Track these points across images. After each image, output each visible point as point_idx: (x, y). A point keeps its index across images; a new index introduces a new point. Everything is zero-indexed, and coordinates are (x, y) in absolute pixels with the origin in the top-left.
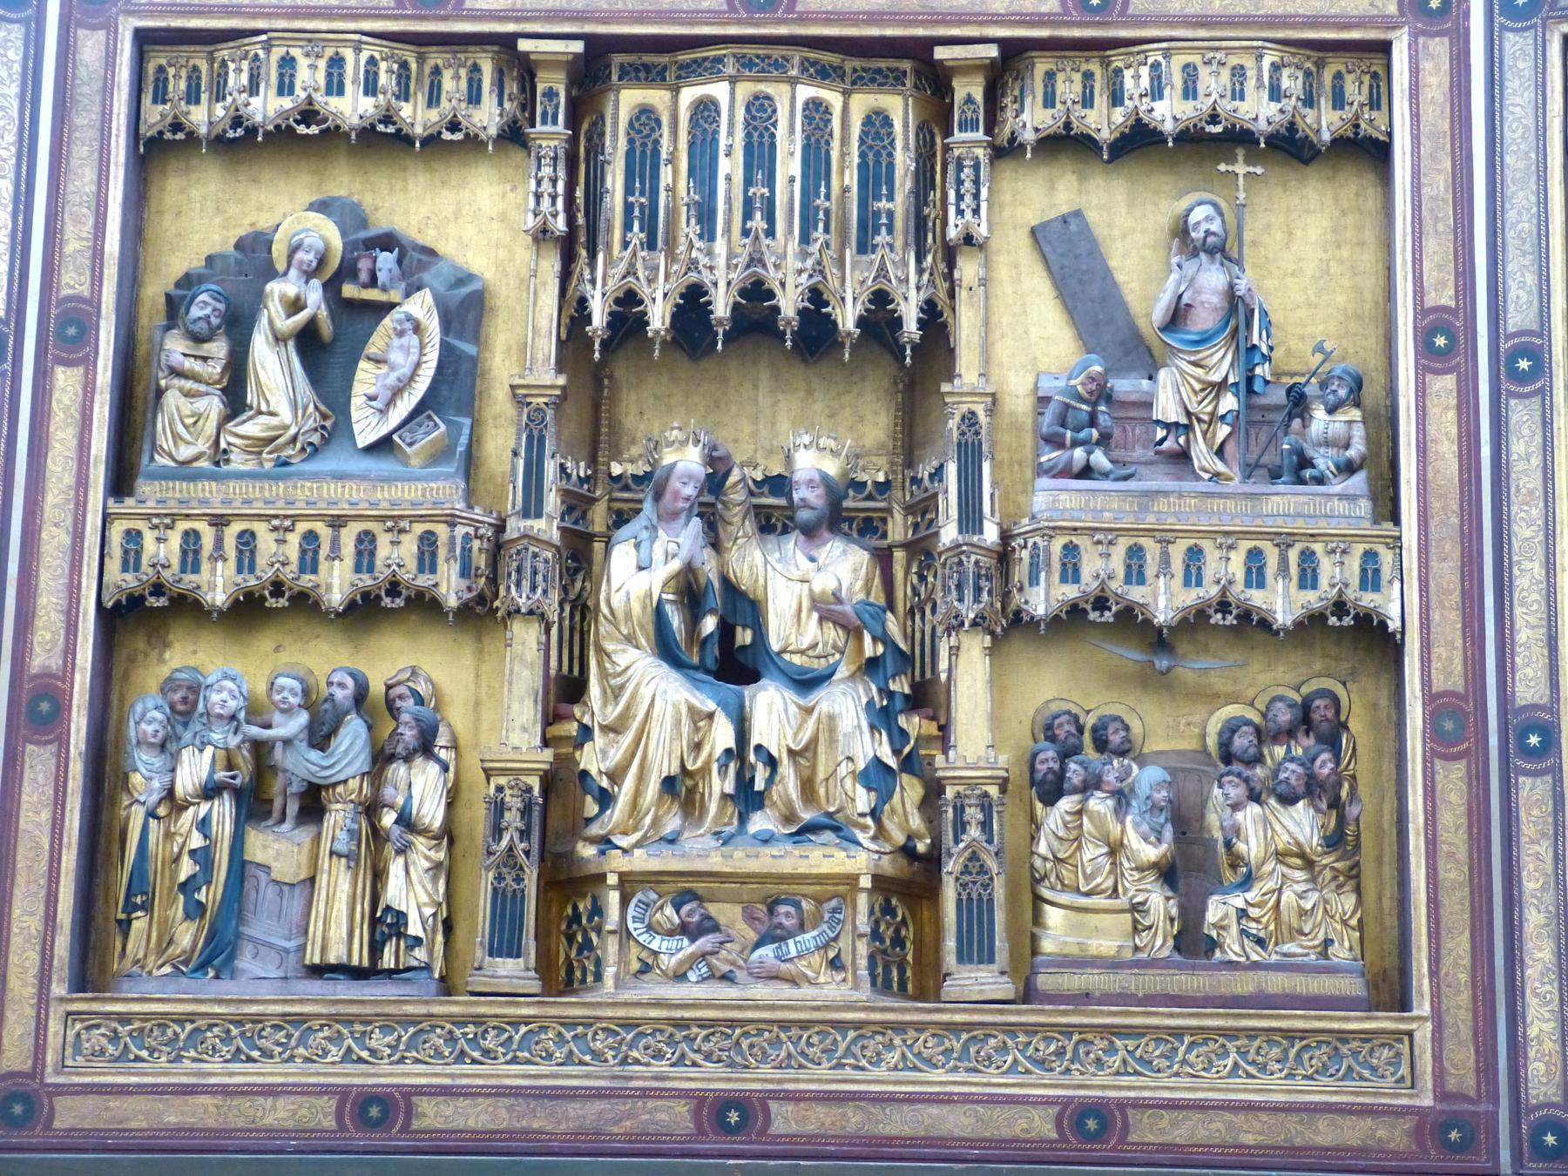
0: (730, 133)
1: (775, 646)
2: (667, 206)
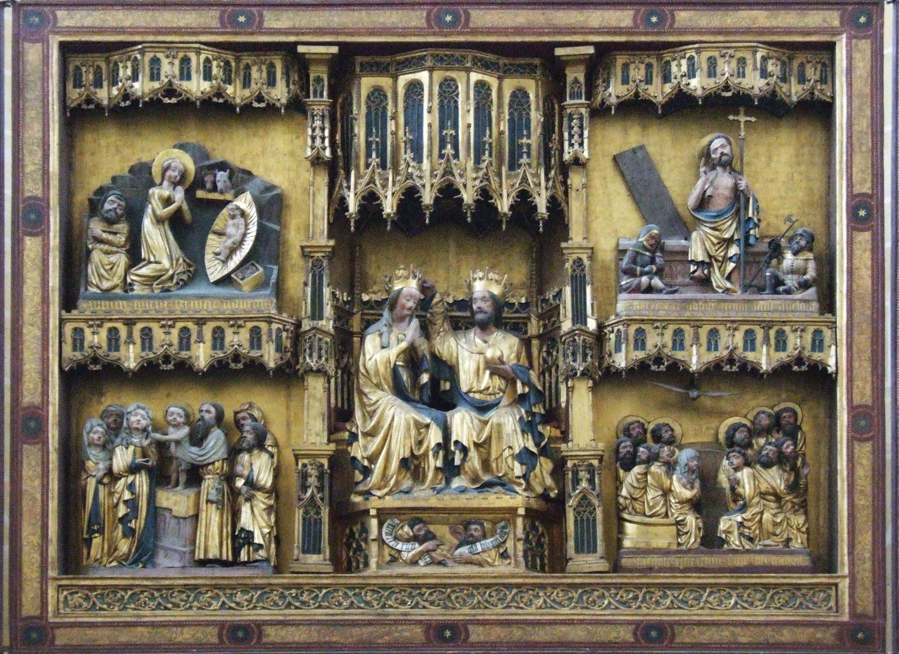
0: (431, 99)
1: (464, 388)
2: (392, 143)
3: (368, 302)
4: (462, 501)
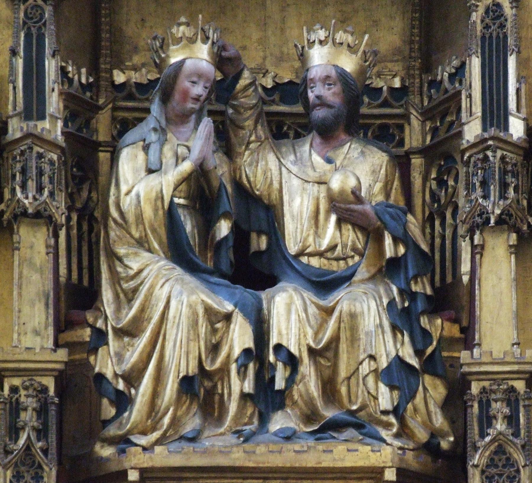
1: (292, 248)
3: (124, 85)
4: (287, 457)
